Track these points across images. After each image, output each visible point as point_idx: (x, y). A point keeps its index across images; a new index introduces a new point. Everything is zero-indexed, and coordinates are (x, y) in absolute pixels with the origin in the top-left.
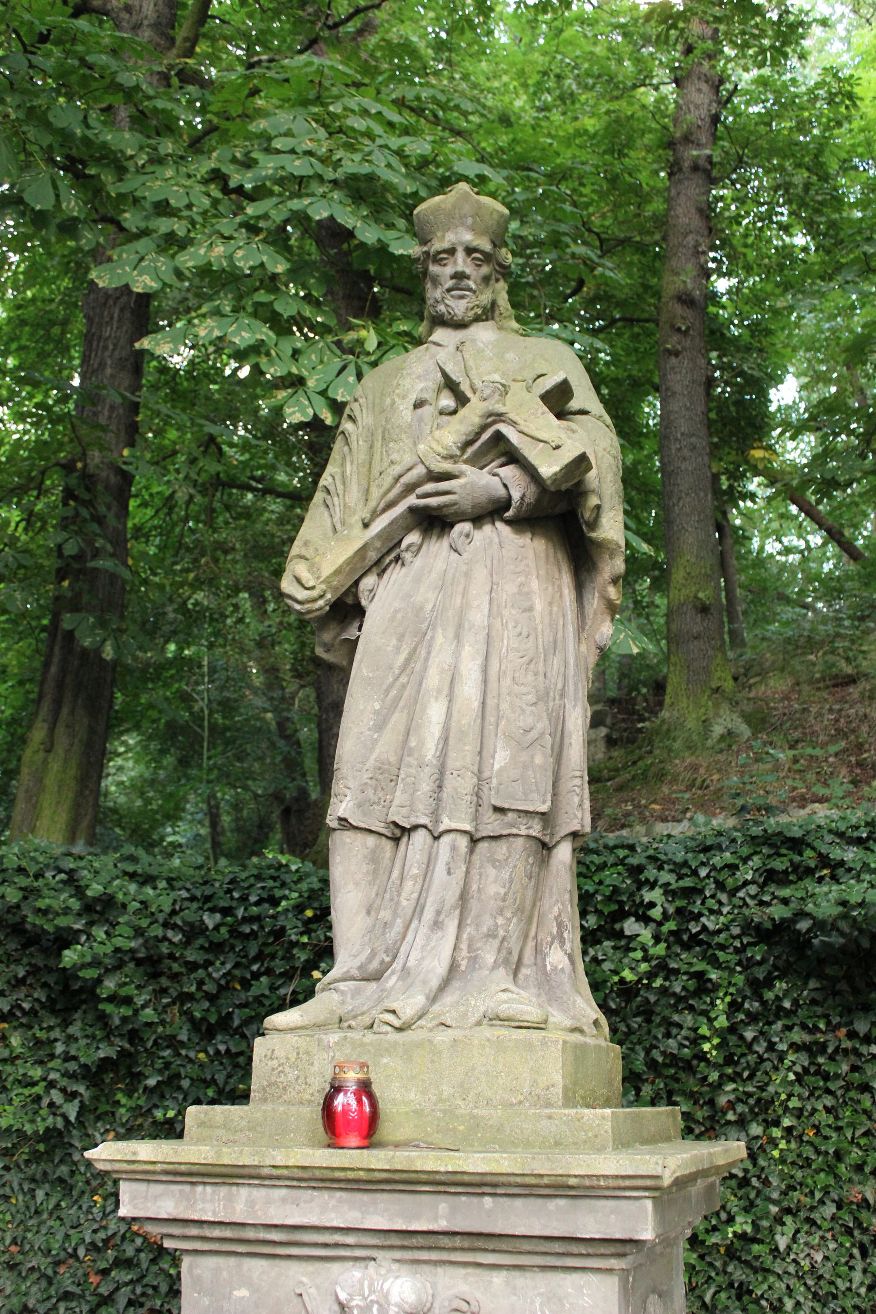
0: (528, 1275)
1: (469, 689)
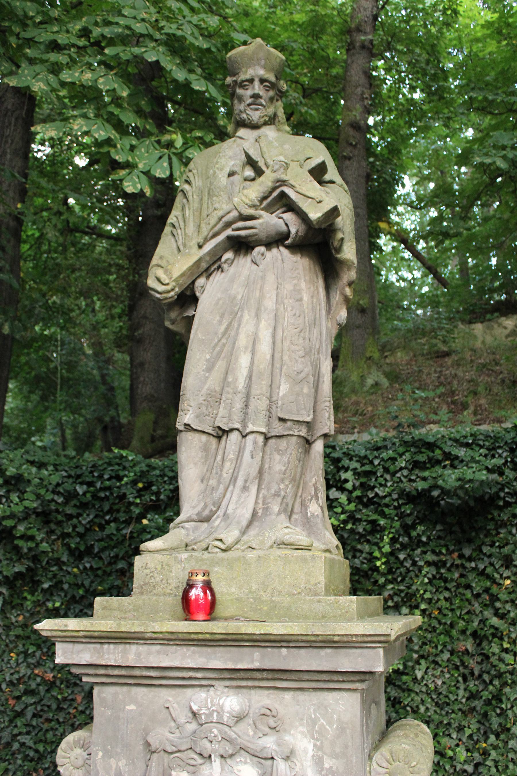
0: (306, 693)
1: (264, 347)
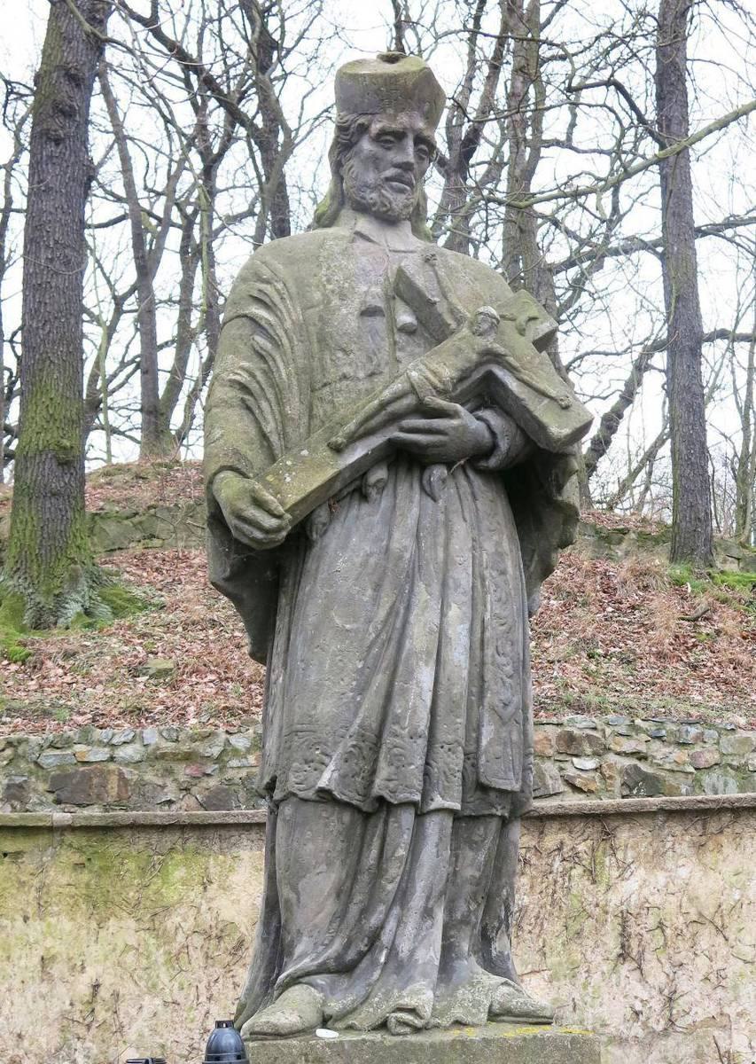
1: (458, 656)
